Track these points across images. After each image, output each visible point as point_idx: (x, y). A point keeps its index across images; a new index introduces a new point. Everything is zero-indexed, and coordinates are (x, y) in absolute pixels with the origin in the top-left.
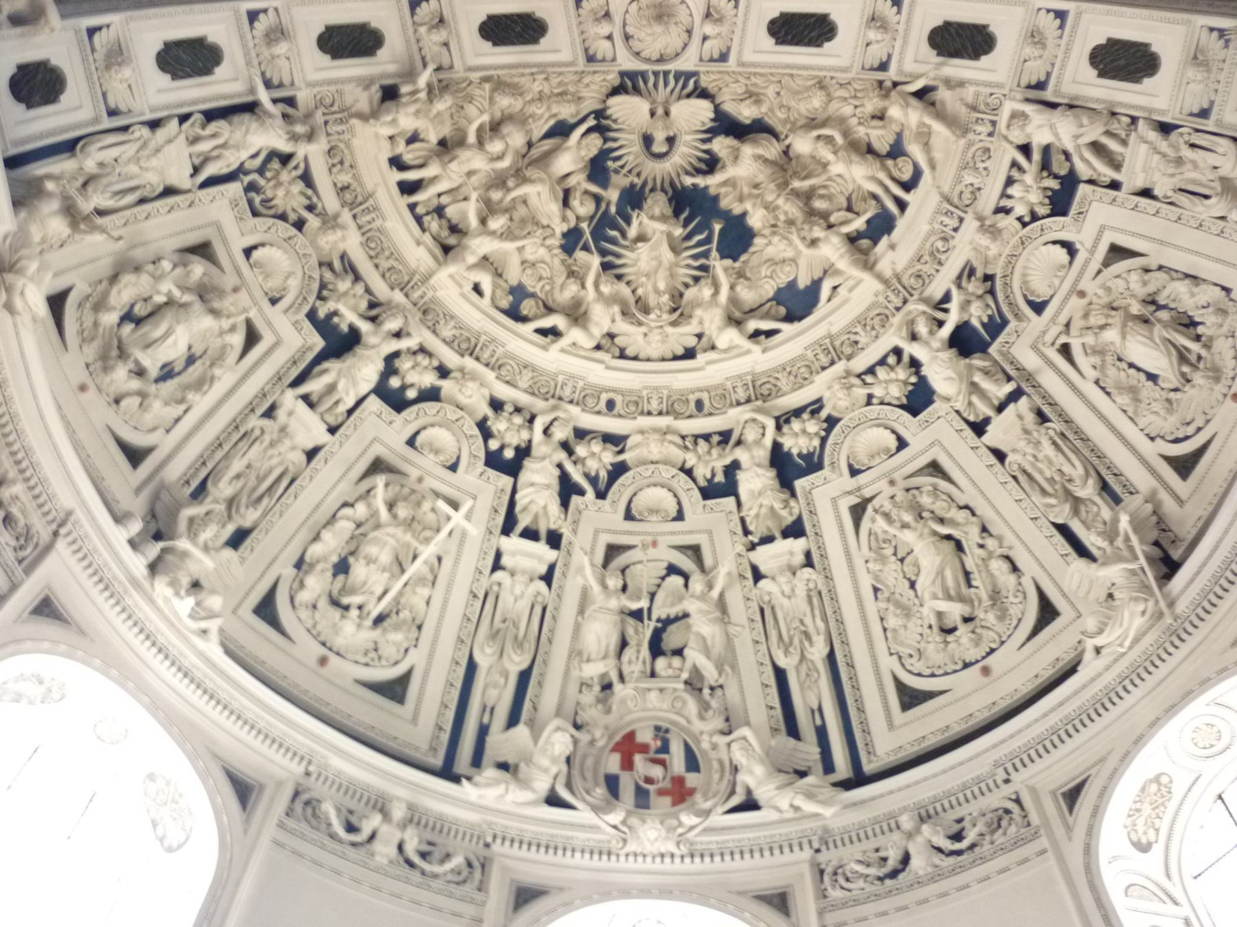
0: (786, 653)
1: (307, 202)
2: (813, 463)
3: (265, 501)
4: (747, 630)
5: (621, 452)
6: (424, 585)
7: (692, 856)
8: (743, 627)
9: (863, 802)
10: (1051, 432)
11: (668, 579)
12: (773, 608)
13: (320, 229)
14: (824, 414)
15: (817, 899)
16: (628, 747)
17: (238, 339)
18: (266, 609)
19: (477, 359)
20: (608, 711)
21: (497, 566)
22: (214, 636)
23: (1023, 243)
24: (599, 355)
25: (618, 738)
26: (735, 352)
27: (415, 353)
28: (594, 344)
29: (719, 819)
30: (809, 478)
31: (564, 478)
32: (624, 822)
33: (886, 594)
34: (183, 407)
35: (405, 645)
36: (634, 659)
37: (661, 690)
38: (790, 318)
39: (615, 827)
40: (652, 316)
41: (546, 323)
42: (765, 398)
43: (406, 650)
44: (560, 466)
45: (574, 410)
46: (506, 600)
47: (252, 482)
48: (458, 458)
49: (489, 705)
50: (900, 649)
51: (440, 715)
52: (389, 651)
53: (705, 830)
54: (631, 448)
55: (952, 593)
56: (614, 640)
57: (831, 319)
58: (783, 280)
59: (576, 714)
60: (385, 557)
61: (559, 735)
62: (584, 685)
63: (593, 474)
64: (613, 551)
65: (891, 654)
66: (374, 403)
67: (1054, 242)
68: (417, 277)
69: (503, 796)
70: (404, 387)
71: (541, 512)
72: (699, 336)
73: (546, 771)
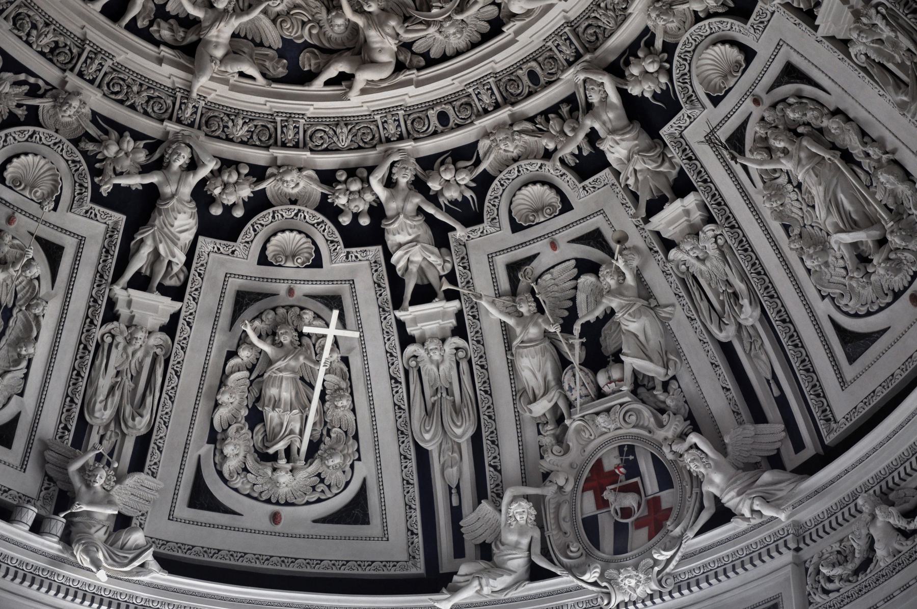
0: (721, 325)
1: (26, 88)
3: (149, 400)
4: (679, 308)
5: (478, 162)
6: (341, 397)
8: (673, 305)
9: (824, 487)
10: (883, 11)
13: (54, 107)
14: (658, 44)
17: (40, 269)
19: (284, 145)
20: (567, 450)
22: (154, 565)
24: (402, 77)
25: (586, 473)
28: (391, 69)
29: (693, 543)
30: (671, 123)
31: (430, 220)
32: (602, 575)
33: (797, 231)
34: (24, 364)
35: (349, 463)
37: (608, 411)
39: (595, 584)
40: (434, 11)
41: (332, 72)
42: (592, 47)
43: (352, 466)
45: (408, 145)
46: (428, 369)
47: (129, 385)
48: (317, 251)
49: (454, 486)
50: (830, 291)
51: (408, 518)
52: (335, 477)
53: (684, 558)
55: (854, 216)
60: (286, 393)
61: (514, 506)
62: (539, 425)
63: (460, 199)
65: (823, 298)
66: (206, 244)
68: (179, 95)
73: (516, 546)
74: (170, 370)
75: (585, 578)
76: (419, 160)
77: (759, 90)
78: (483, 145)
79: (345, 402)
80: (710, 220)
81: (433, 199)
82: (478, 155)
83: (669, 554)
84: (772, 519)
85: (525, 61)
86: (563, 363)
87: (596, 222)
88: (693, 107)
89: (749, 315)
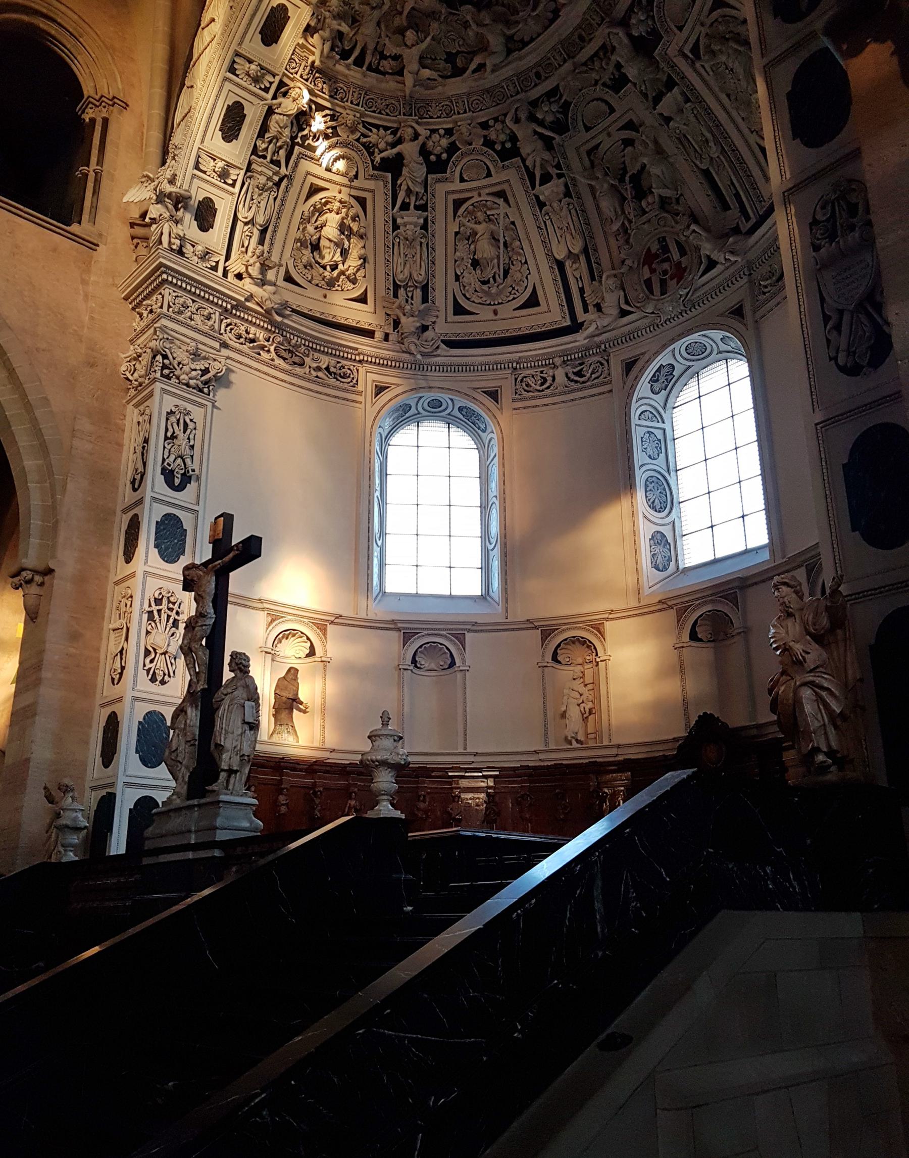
2: (654, 37)
5: (561, 96)
12: (685, 136)
18: (459, 310)
21: (541, 205)
22: (443, 346)
24: (510, 58)
27: (430, 136)
37: (649, 221)
39: (653, 313)
41: (473, 66)
43: (527, 278)
53: (695, 290)
65: (752, 132)
70: (438, 156)
74: (430, 249)
80: (687, 100)
81: (541, 123)
84: (736, 261)
85: (576, 29)
86: (623, 199)
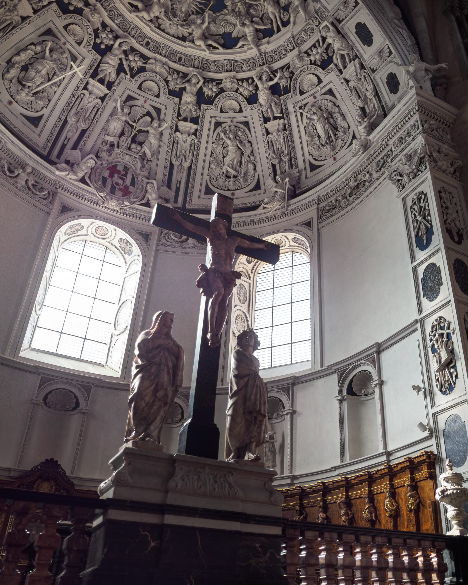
5: (145, 63)
7: (124, 214)
11: (146, 117)
15: (157, 241)
16: (113, 169)
20: (110, 156)
23: (307, 69)
25: (111, 165)
26: (200, 48)
29: (136, 206)
32: (105, 197)
36: (124, 141)
37: (130, 156)
38: (224, 46)
39: (101, 197)
43: (42, 108)
44: (121, 59)
46: (85, 101)
49: (68, 138)
54: (149, 64)
56: (120, 131)
57: (238, 55)
58: (228, 29)
59: (98, 152)
61: (91, 160)
62: (104, 142)
63: (132, 67)
64: (130, 98)
67: (316, 76)
69: (66, 175)
71: (108, 74)
72: (190, 34)
73: (83, 171)
75: (99, 193)
76: (131, 47)
77: (235, 120)
78: (150, 61)
79: (56, 89)
81: (126, 60)
82: (148, 61)
83: (129, 204)
87: (163, 108)
88: (215, 107)
89: (187, 164)
